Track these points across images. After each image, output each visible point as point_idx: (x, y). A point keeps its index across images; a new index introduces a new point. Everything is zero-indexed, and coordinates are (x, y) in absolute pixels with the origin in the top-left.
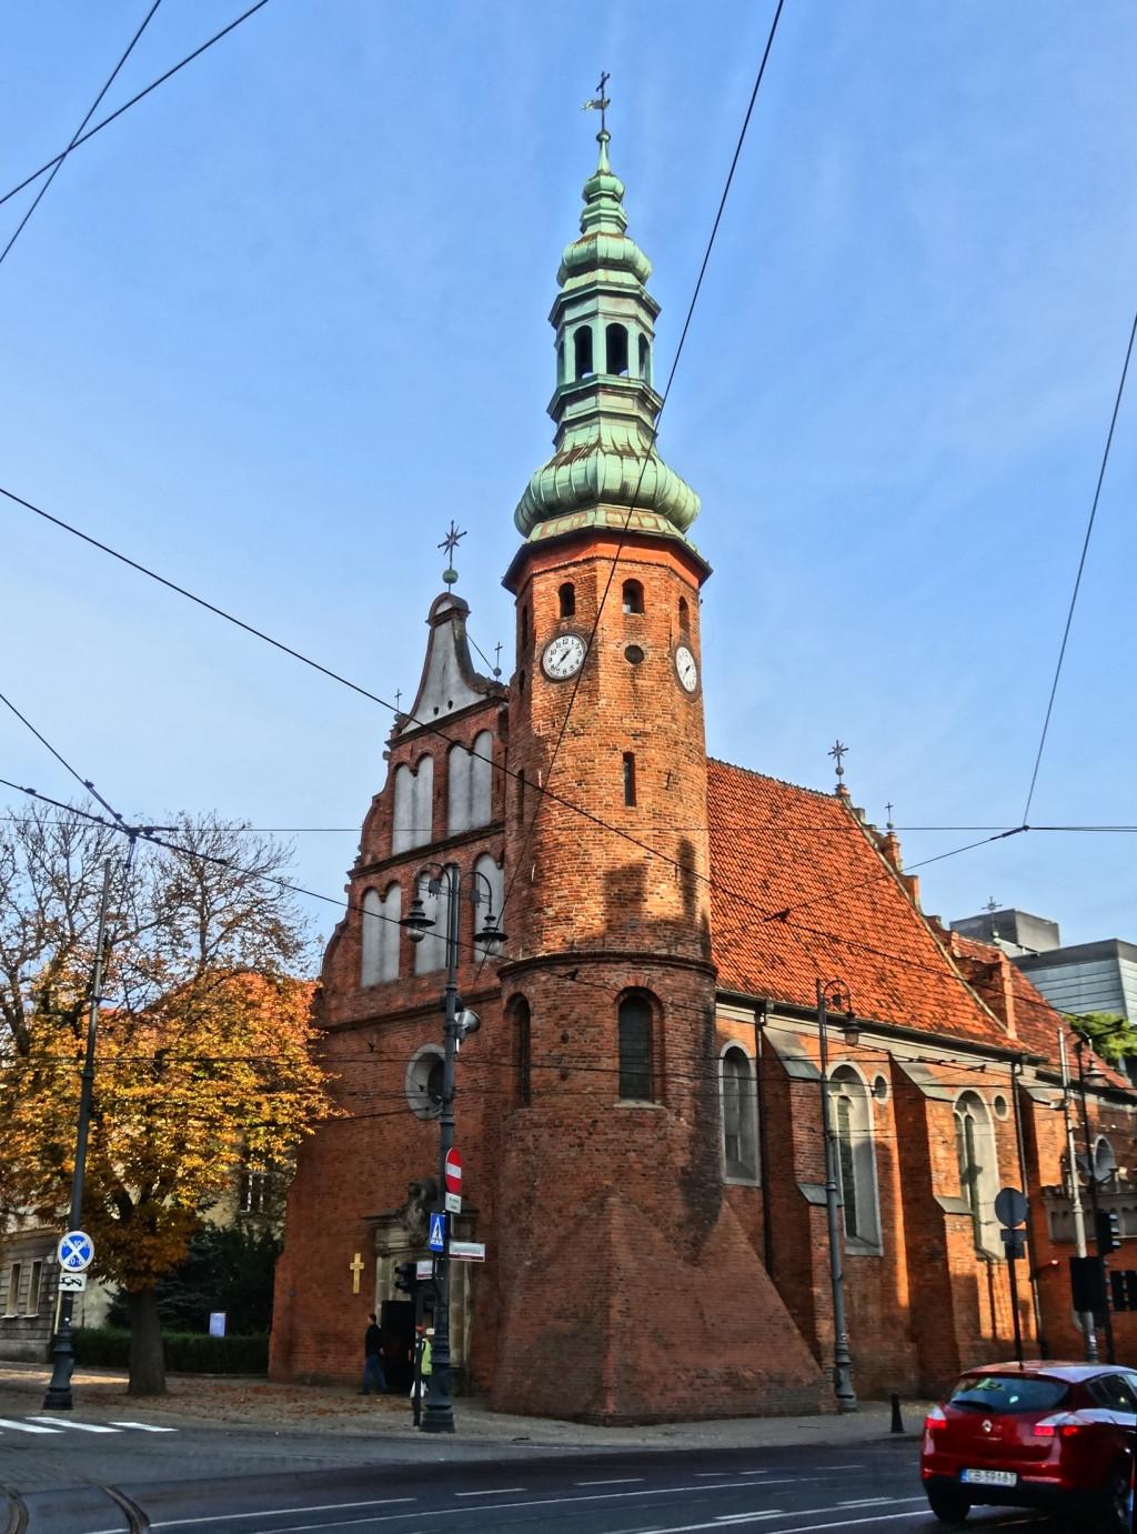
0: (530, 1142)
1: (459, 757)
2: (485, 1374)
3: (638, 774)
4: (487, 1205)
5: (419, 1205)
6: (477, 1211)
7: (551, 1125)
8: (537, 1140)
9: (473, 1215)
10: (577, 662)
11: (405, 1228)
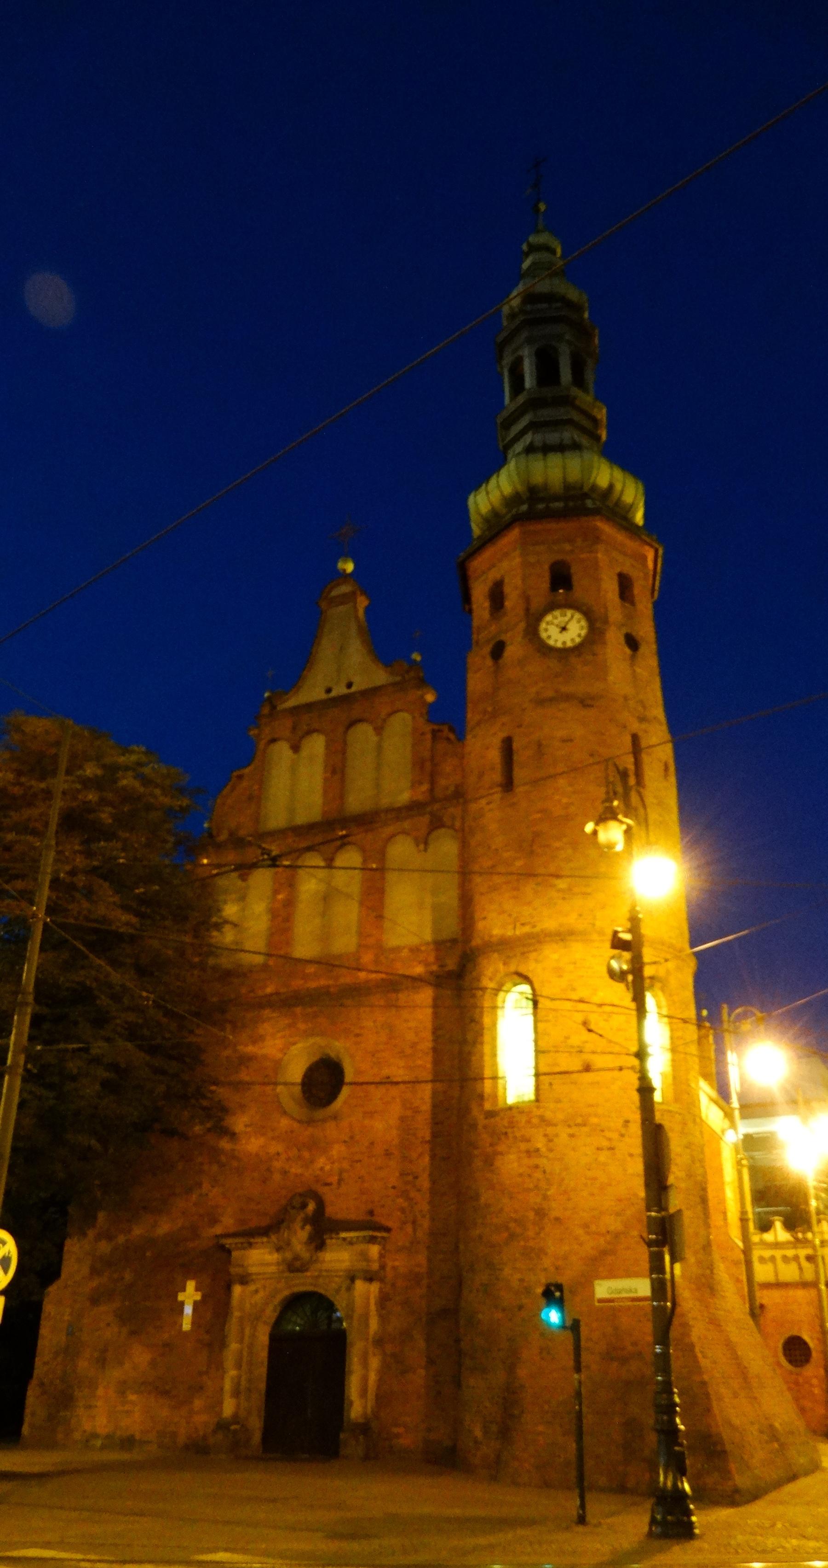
0: (540, 1143)
1: (363, 734)
2: (401, 1430)
3: (645, 758)
4: (404, 1223)
5: (306, 1221)
6: (388, 1230)
7: (568, 1123)
8: (551, 1141)
9: (385, 1234)
10: (579, 635)
11: (278, 1249)
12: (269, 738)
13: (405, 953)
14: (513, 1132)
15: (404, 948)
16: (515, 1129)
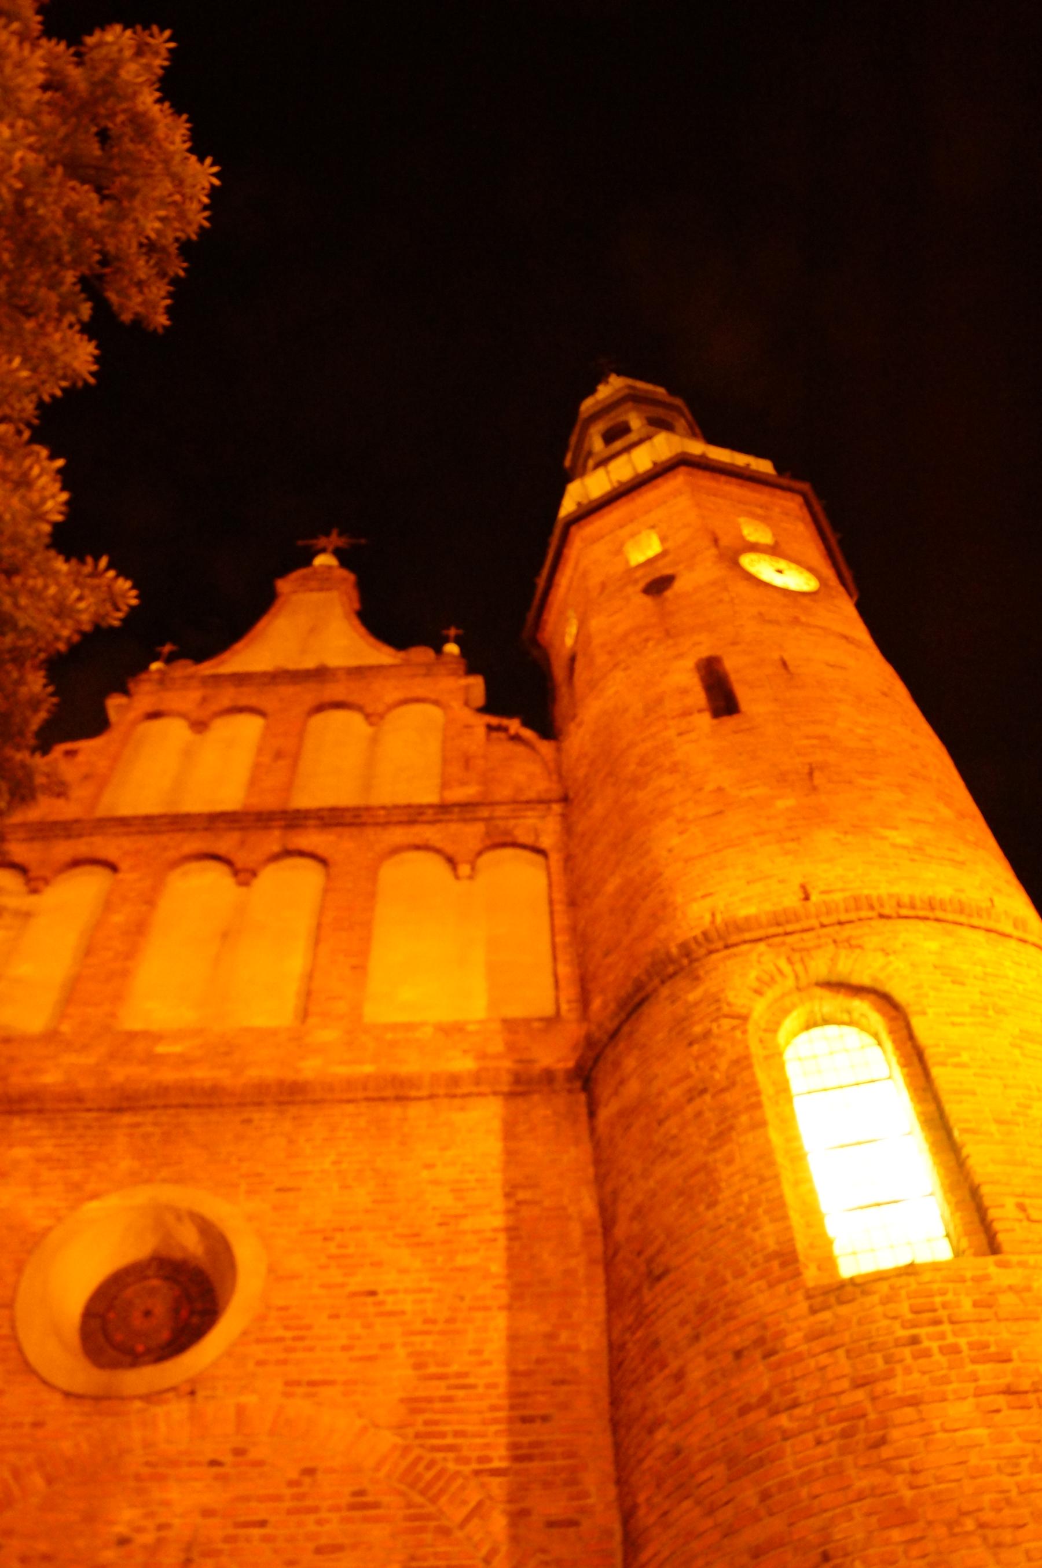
12: (149, 709)
13: (429, 1030)
14: (942, 1336)
15: (423, 1024)
16: (946, 1327)
